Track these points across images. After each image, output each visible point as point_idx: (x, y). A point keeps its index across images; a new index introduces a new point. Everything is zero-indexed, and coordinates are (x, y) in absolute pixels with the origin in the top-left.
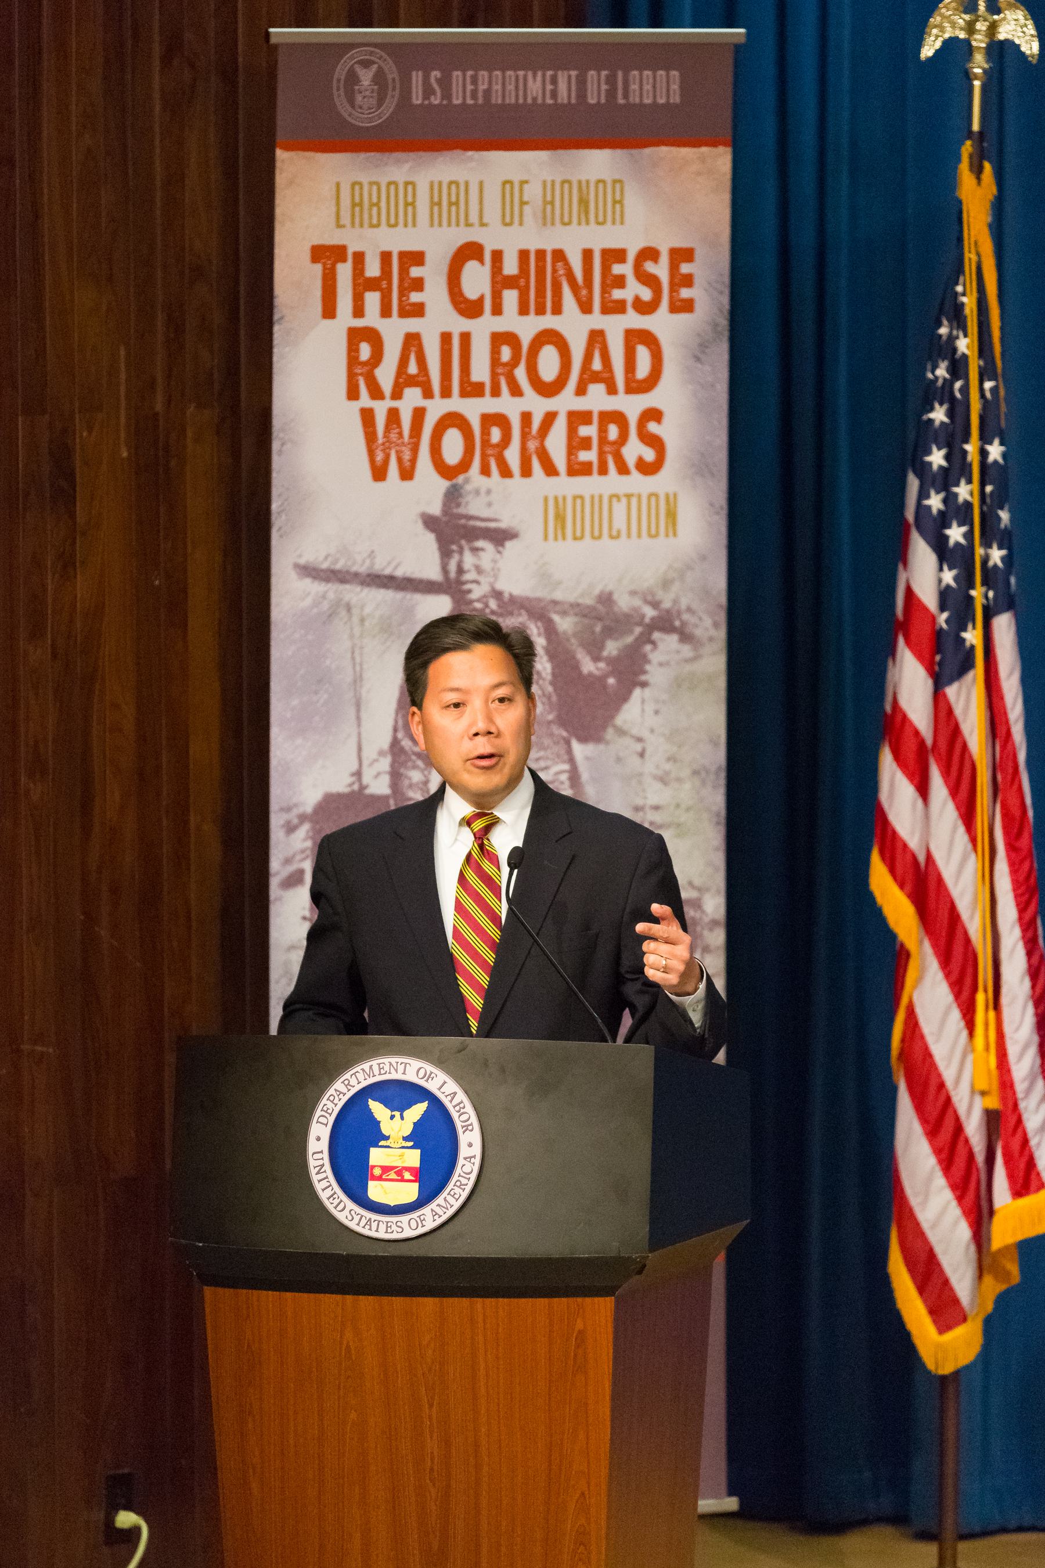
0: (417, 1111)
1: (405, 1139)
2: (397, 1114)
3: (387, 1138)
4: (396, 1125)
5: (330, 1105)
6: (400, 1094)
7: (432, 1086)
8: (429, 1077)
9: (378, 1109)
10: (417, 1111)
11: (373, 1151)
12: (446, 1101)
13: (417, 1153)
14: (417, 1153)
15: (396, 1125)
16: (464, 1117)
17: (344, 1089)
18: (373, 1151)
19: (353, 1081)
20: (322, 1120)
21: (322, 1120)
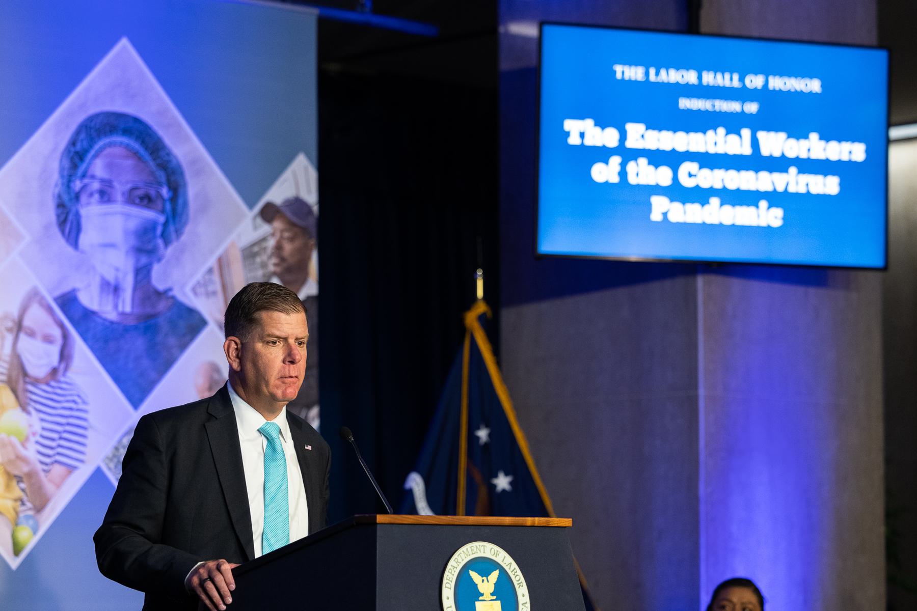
0: (494, 576)
1: (492, 594)
2: (485, 578)
3: (482, 595)
4: (486, 585)
5: (450, 575)
6: (484, 566)
7: (499, 559)
8: (496, 554)
9: (475, 576)
10: (494, 576)
11: (477, 603)
12: (507, 568)
13: (499, 602)
14: (499, 602)
15: (486, 585)
16: (518, 578)
17: (455, 565)
18: (477, 603)
19: (460, 560)
20: (448, 585)
21: (448, 585)
